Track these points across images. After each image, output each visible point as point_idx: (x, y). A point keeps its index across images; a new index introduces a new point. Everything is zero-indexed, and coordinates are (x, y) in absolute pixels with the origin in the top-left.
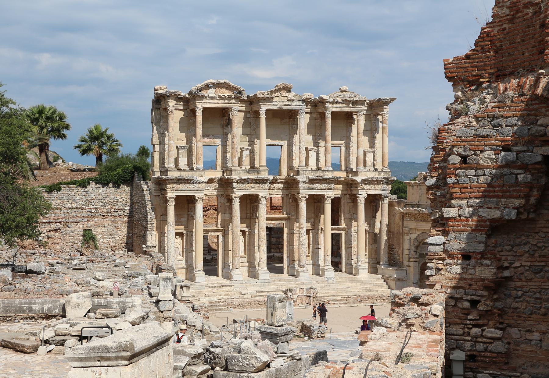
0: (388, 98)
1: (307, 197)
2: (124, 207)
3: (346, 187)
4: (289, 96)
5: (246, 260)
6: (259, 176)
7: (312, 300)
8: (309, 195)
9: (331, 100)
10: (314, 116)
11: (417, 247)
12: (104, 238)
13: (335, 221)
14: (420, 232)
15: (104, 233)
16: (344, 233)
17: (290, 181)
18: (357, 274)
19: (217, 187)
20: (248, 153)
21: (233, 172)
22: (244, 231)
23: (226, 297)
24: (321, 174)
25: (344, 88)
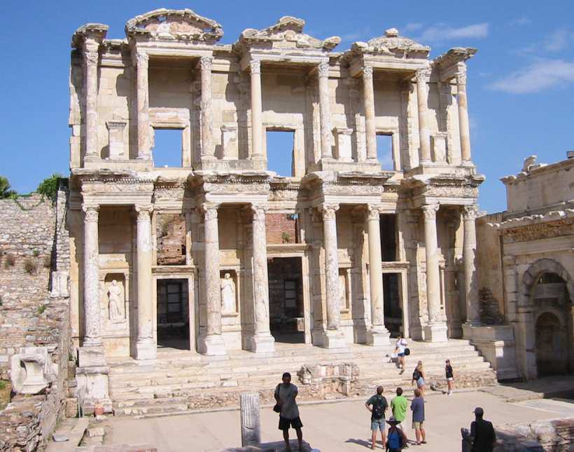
0: (464, 49)
1: (338, 208)
2: (45, 242)
3: (404, 196)
4: (299, 41)
5: (238, 320)
6: (251, 171)
7: (348, 387)
8: (341, 205)
9: (372, 49)
10: (347, 82)
11: (529, 287)
12: (11, 292)
13: (389, 252)
14: (535, 260)
15: (10, 284)
16: (404, 273)
17: (308, 186)
18: (429, 339)
19: (182, 196)
20: (234, 135)
21: (204, 166)
22: (234, 270)
23: (190, 386)
24: (360, 170)
25: (393, 31)
